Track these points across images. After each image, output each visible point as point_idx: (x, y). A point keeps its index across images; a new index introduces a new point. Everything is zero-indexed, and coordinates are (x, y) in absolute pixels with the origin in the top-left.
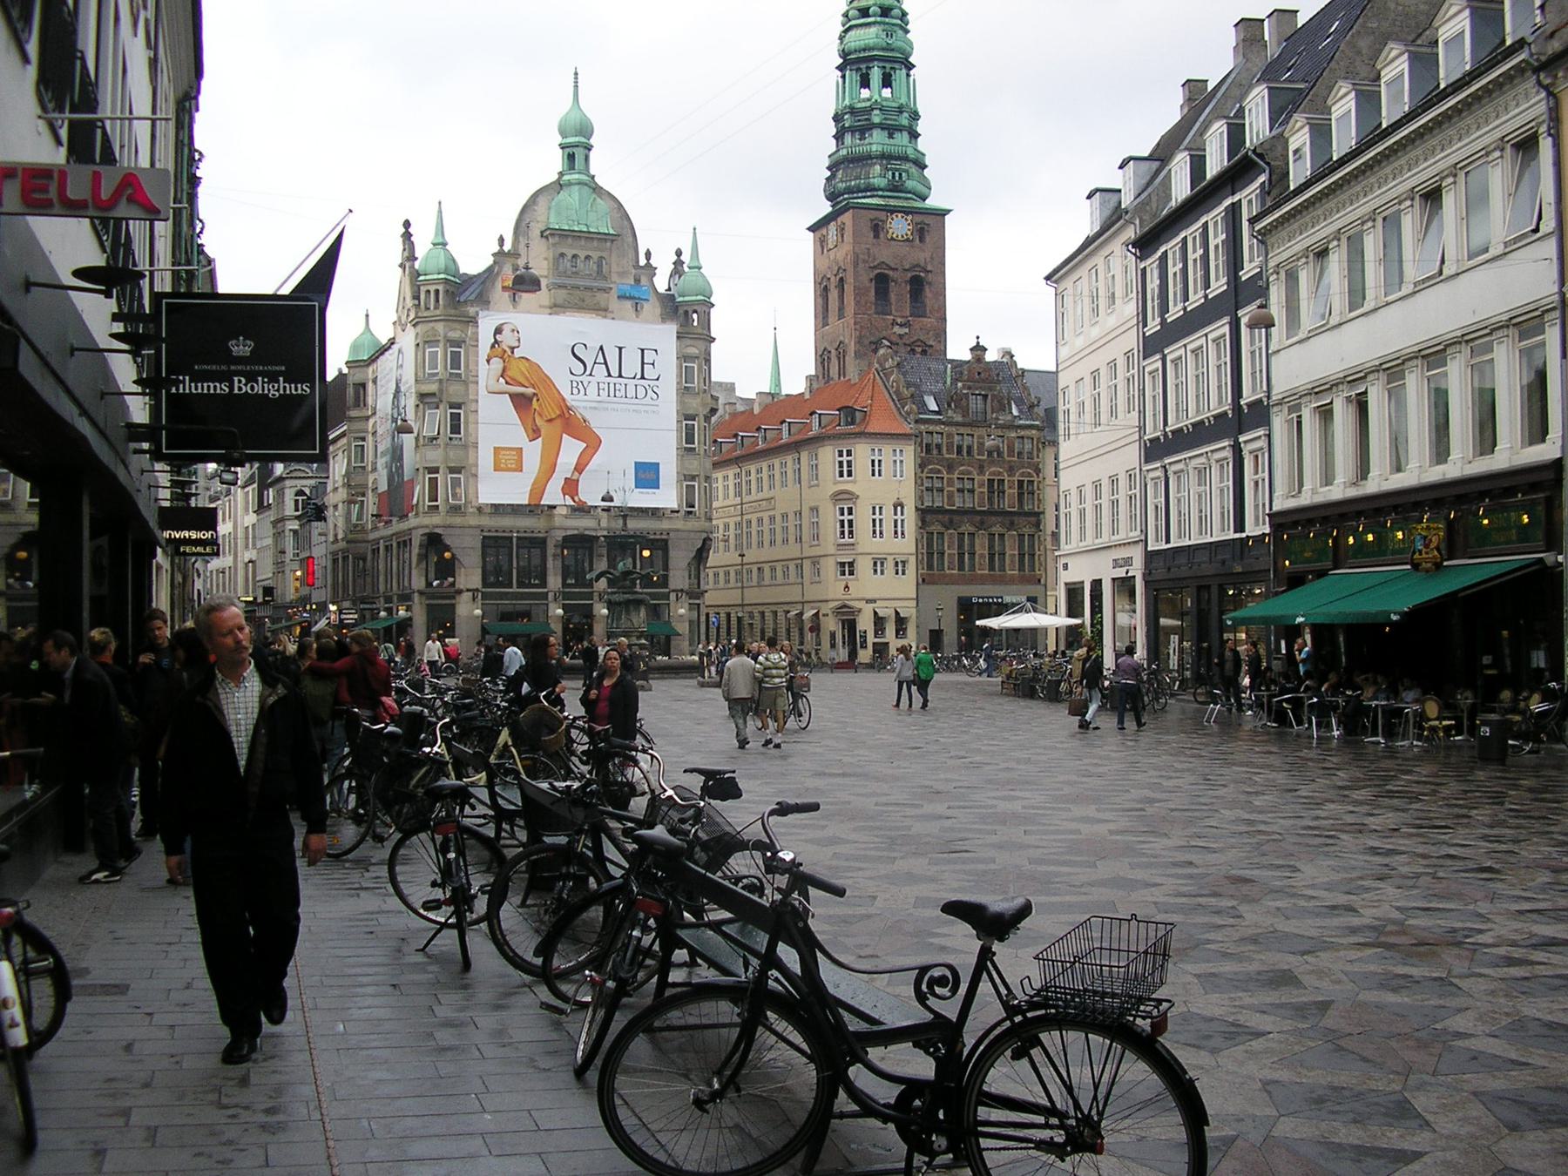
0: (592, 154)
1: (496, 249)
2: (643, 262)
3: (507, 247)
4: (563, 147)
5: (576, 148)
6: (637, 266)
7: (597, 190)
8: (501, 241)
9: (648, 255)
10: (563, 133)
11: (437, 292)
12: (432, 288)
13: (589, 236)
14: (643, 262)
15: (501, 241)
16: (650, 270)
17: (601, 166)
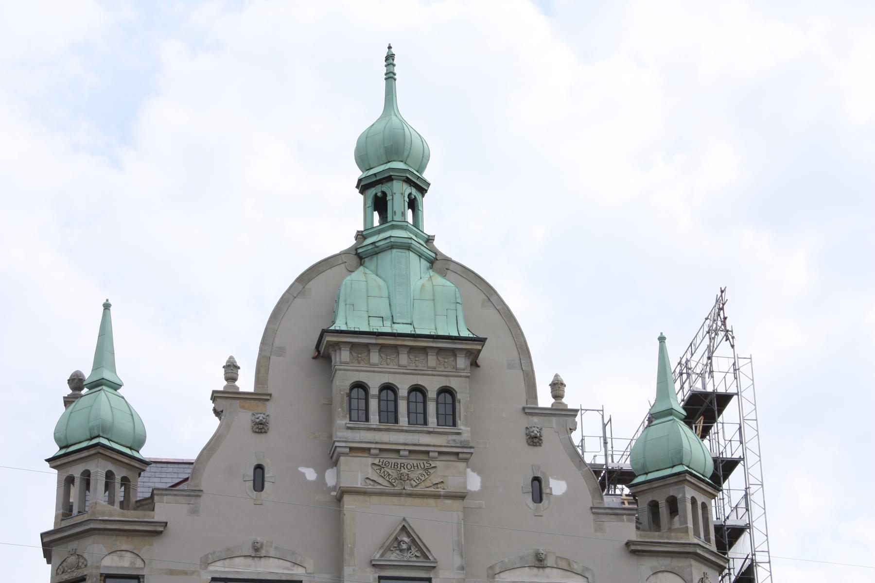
0: (427, 202)
1: (221, 384)
2: (545, 400)
3: (246, 383)
4: (363, 186)
5: (390, 179)
6: (531, 410)
7: (437, 262)
8: (231, 370)
9: (557, 387)
10: (362, 159)
11: (87, 474)
12: (77, 471)
13: (420, 345)
14: (545, 400)
15: (231, 370)
16: (565, 416)
17: (449, 220)
